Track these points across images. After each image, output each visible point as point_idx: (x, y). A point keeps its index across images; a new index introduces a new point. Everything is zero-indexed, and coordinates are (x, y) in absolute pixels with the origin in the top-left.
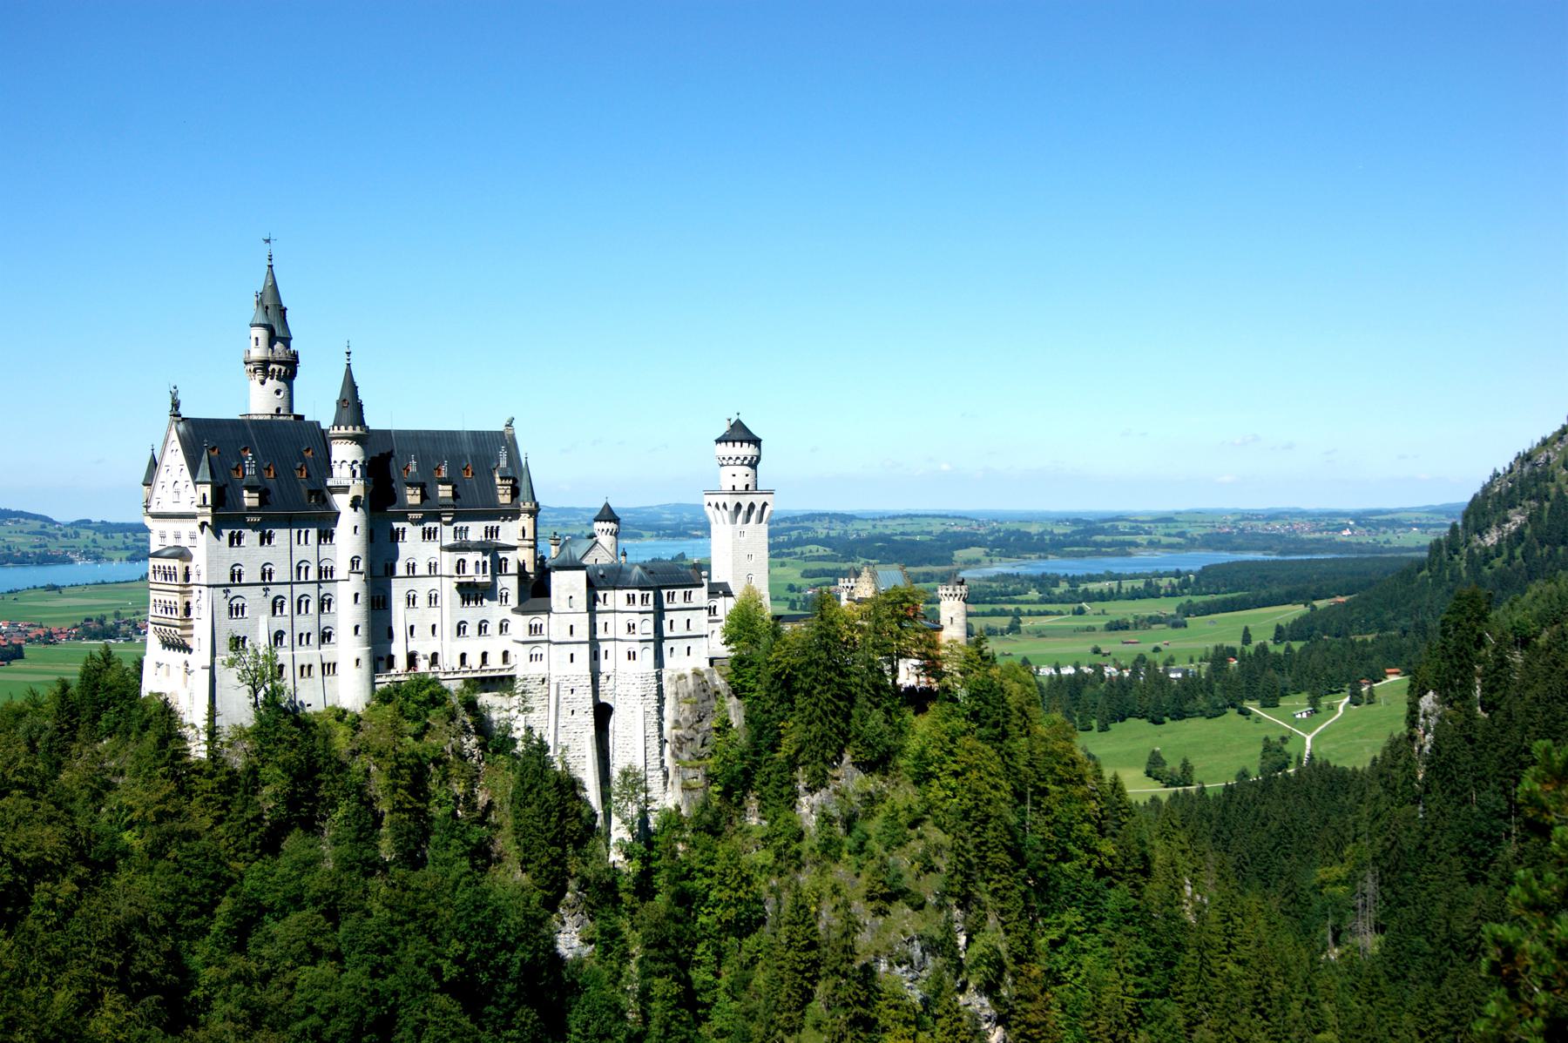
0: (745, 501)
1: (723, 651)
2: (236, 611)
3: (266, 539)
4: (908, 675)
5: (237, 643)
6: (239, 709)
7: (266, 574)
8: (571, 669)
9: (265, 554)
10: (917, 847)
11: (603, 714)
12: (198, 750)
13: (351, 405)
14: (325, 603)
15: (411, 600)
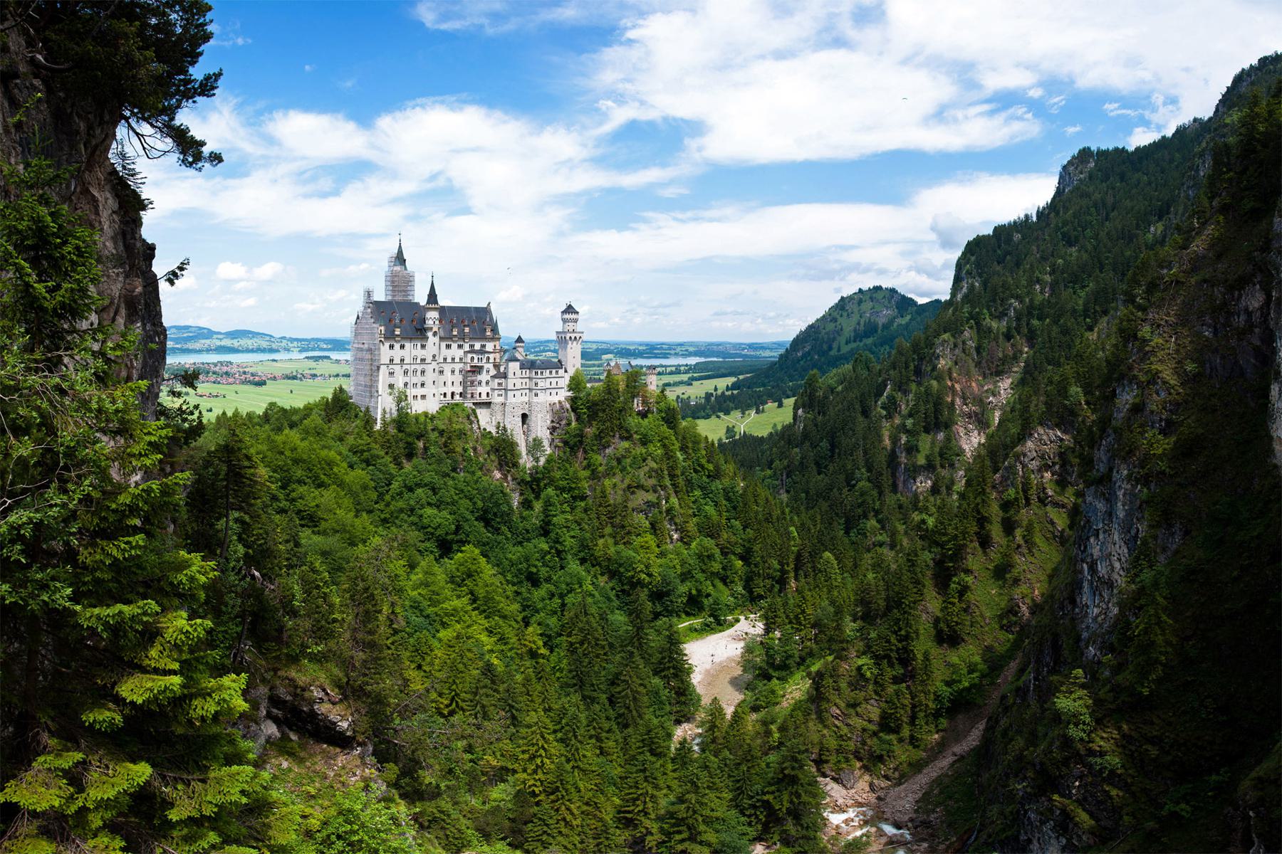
0: (573, 336)
1: (569, 394)
2: (391, 374)
3: (402, 347)
4: (637, 405)
5: (391, 386)
6: (395, 414)
7: (402, 360)
8: (514, 400)
9: (402, 352)
10: (646, 469)
11: (524, 417)
12: (378, 427)
13: (432, 296)
14: (423, 372)
15: (453, 372)
